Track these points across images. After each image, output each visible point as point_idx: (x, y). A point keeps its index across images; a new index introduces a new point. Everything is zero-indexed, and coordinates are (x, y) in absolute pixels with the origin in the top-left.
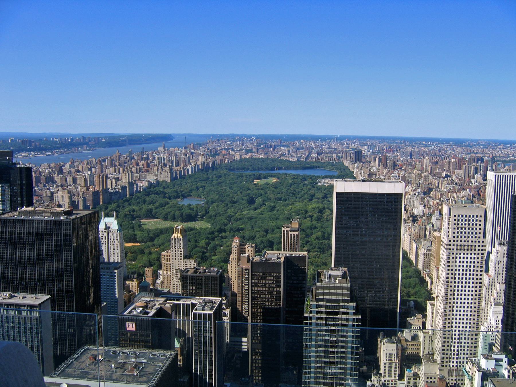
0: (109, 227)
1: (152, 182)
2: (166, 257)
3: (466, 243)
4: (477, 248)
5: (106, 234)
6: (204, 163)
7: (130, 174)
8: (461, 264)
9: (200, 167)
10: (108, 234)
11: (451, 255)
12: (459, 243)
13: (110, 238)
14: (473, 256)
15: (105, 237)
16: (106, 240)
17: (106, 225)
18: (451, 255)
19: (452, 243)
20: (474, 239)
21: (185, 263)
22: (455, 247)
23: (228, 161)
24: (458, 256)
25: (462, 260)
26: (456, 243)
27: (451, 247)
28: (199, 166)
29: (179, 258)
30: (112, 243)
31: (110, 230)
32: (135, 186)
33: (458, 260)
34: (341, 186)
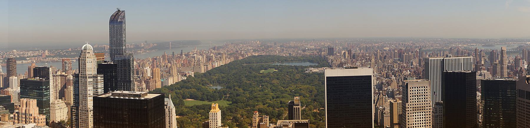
3: (419, 106)
4: (426, 108)
8: (417, 120)
11: (410, 115)
12: (414, 106)
14: (424, 113)
18: (410, 115)
19: (410, 106)
20: (424, 102)
22: (412, 109)
24: (414, 114)
25: (417, 117)
26: (412, 106)
27: (410, 109)
33: (414, 117)
34: (329, 73)
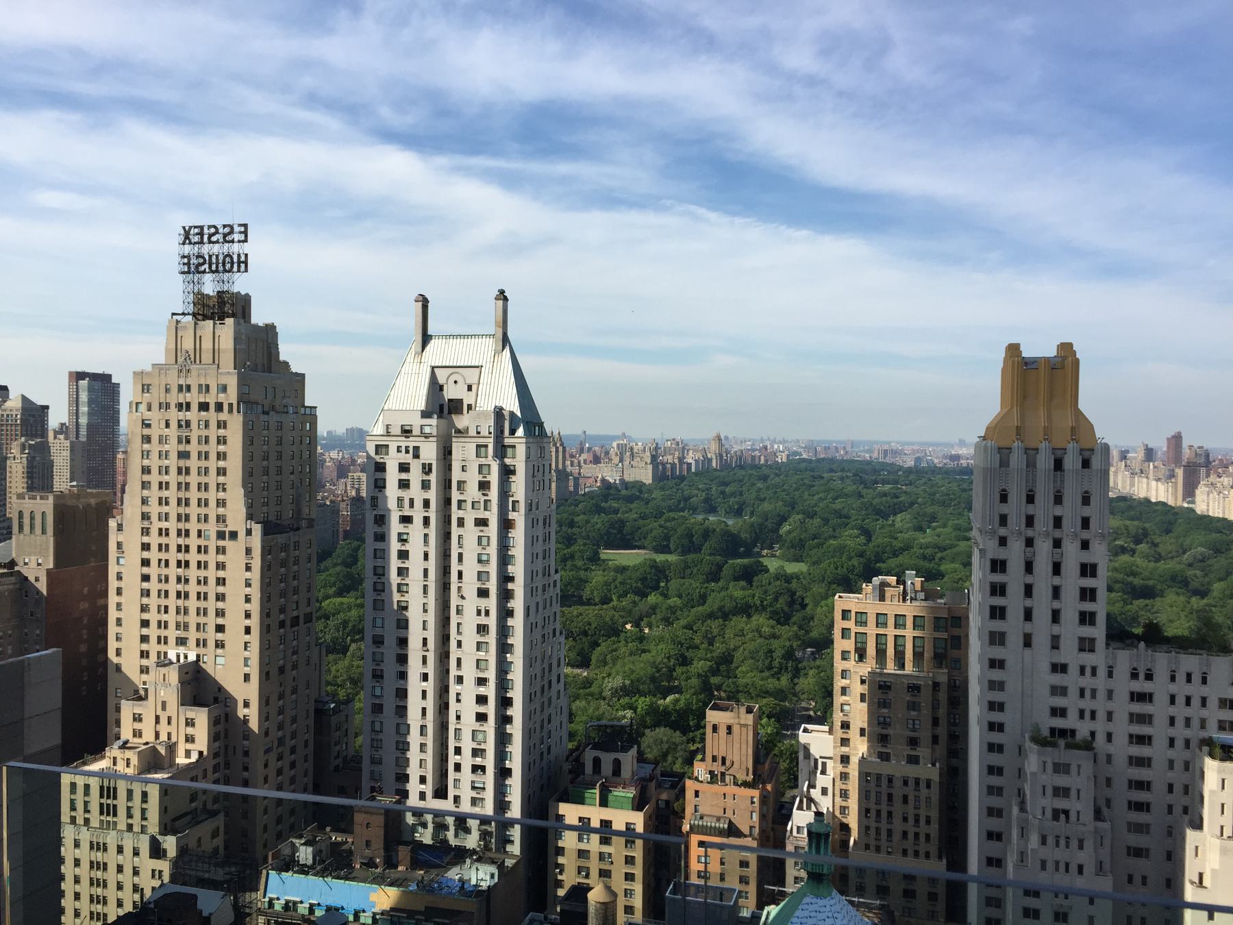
0: (456, 406)
1: (612, 481)
2: (871, 630)
5: (429, 452)
6: (721, 456)
7: (561, 449)
9: (714, 465)
10: (446, 453)
13: (456, 475)
15: (427, 469)
16: (432, 495)
17: (436, 387)
21: (1124, 685)
23: (766, 461)
28: (710, 460)
29: (1070, 630)
30: (470, 516)
31: (461, 421)
32: (571, 483)
